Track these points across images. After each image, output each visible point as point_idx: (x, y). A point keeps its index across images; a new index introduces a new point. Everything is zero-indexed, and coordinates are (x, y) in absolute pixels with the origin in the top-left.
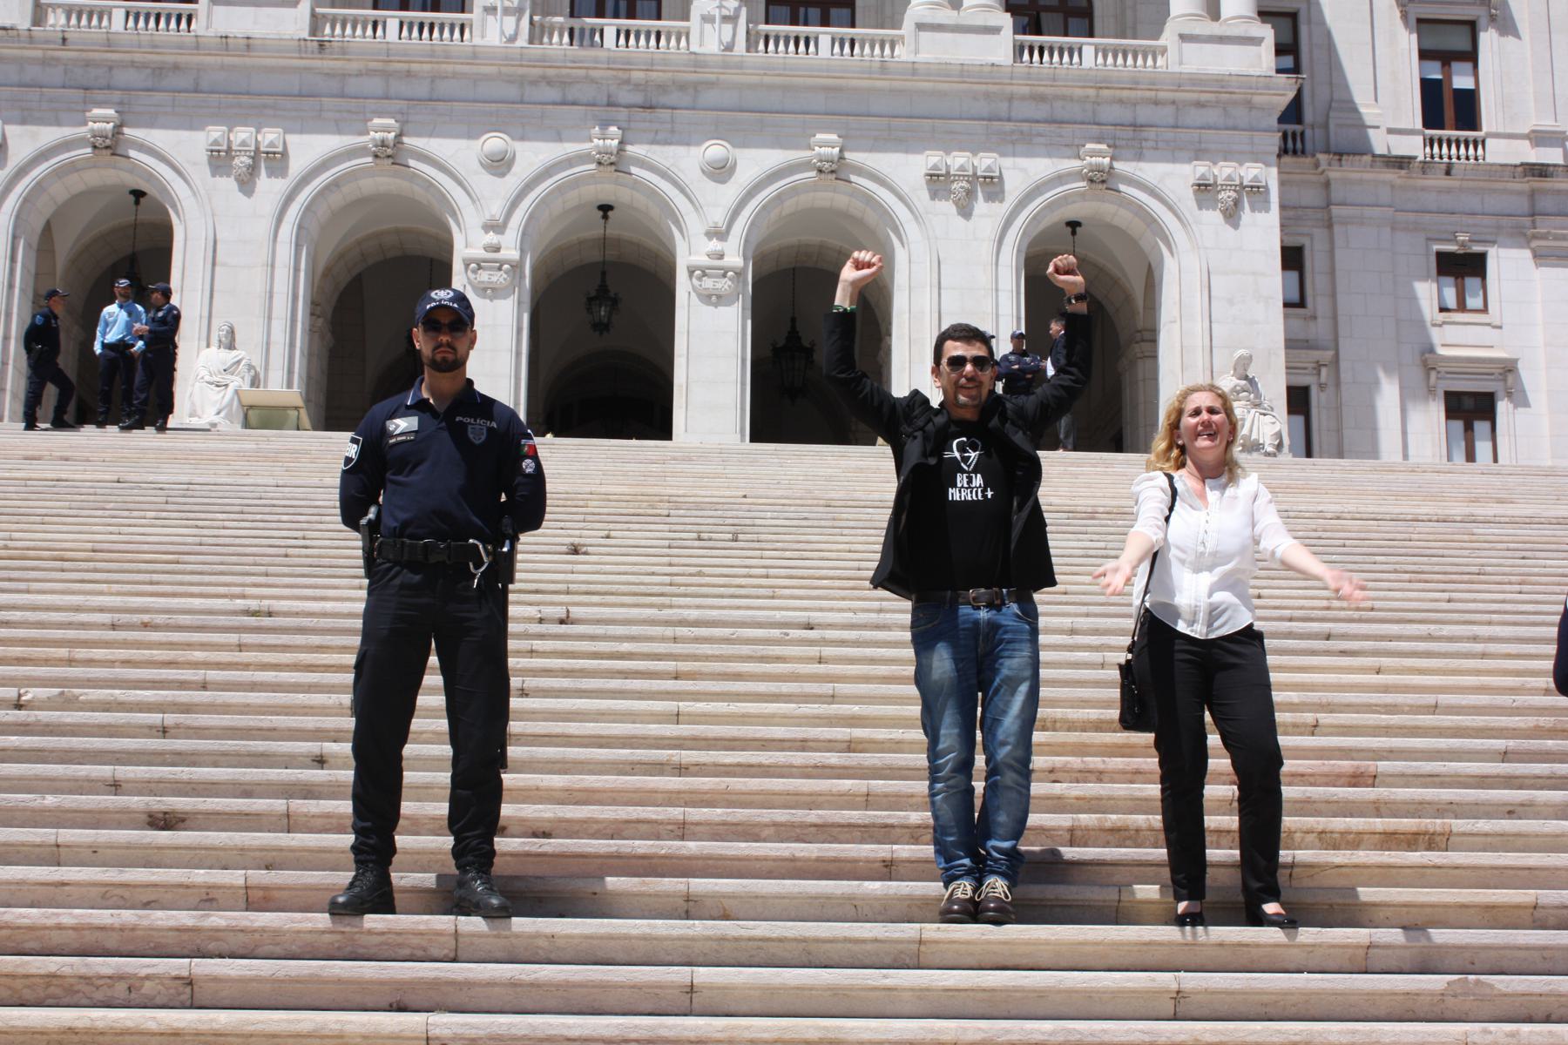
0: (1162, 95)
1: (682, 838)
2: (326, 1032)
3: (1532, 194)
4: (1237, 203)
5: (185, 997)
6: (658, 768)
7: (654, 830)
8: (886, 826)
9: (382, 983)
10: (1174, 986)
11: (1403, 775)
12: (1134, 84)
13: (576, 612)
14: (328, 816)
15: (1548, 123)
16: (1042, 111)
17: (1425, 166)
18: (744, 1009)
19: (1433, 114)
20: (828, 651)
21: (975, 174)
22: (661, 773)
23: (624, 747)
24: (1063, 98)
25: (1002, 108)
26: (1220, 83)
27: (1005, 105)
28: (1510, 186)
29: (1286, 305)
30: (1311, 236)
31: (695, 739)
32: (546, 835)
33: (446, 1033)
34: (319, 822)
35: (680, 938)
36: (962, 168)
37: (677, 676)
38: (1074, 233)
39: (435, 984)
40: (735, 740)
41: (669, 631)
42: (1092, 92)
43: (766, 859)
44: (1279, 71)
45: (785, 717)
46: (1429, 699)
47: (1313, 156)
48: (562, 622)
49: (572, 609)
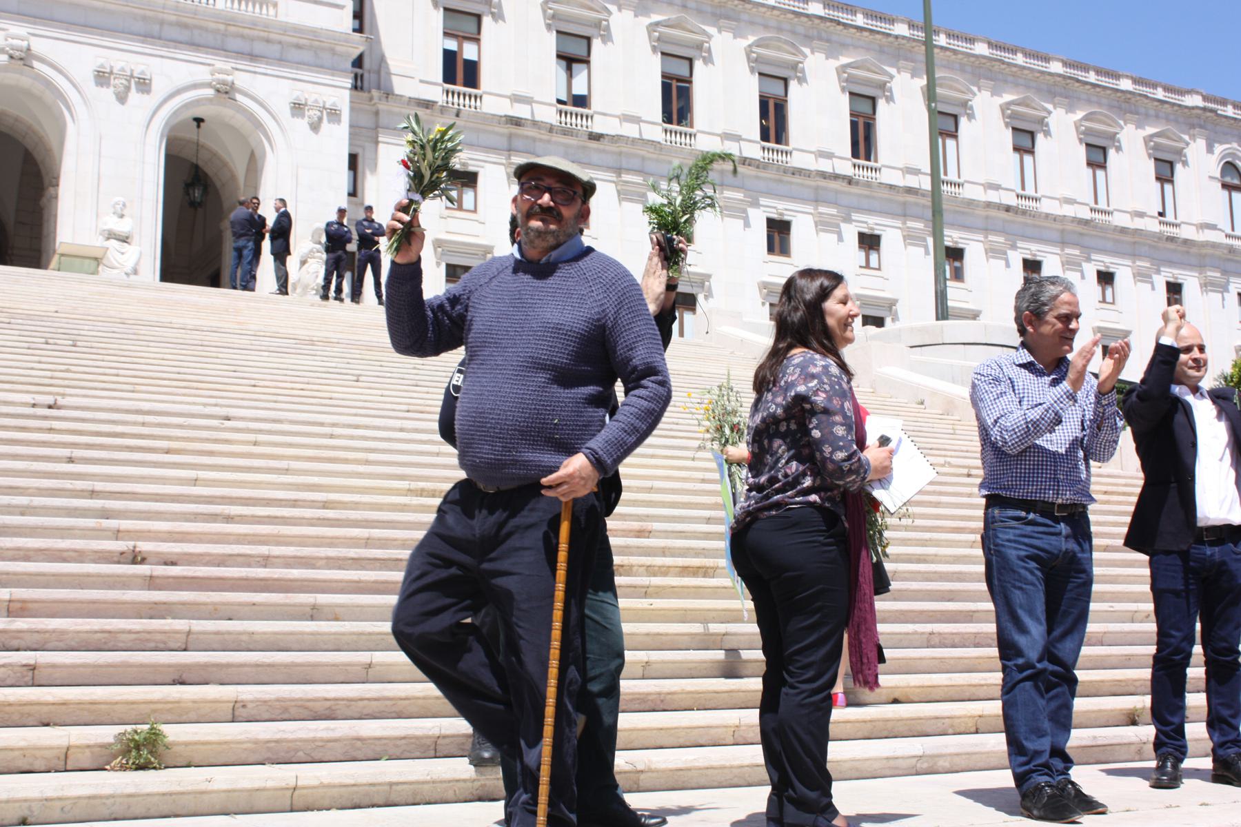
0: (272, 36)
1: (265, 566)
2: (170, 699)
3: (510, 136)
4: (320, 119)
5: (28, 679)
6: (213, 518)
7: (247, 561)
8: (397, 560)
9: (169, 666)
10: (646, 659)
11: (666, 531)
12: (254, 24)
13: (61, 401)
14: (18, 549)
15: (522, 91)
16: (185, 35)
17: (443, 110)
18: (400, 678)
19: (449, 77)
20: (261, 437)
21: (132, 76)
22: (215, 521)
23: (173, 501)
24: (201, 28)
25: (156, 28)
26: (314, 33)
27: (156, 28)
28: (497, 129)
29: (350, 195)
30: (363, 148)
31: (223, 497)
32: (173, 564)
33: (250, 697)
34: (10, 553)
35: (335, 634)
36: (123, 69)
37: (168, 452)
38: (199, 126)
39: (206, 666)
40: (250, 499)
41: (140, 418)
42: (222, 27)
43: (341, 581)
44: (354, 30)
45: (269, 483)
46: (648, 484)
47: (369, 92)
48: (50, 407)
49: (59, 398)
